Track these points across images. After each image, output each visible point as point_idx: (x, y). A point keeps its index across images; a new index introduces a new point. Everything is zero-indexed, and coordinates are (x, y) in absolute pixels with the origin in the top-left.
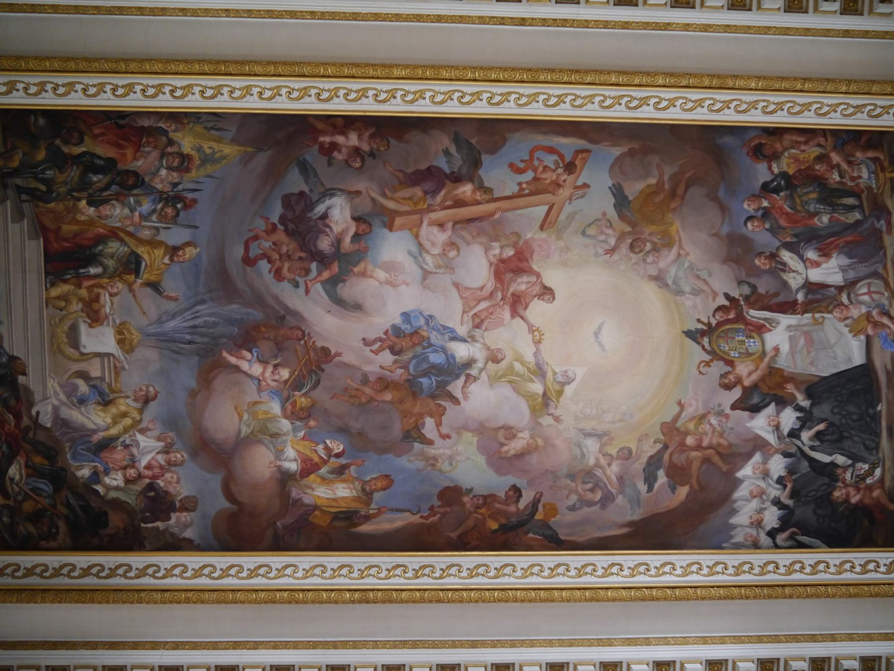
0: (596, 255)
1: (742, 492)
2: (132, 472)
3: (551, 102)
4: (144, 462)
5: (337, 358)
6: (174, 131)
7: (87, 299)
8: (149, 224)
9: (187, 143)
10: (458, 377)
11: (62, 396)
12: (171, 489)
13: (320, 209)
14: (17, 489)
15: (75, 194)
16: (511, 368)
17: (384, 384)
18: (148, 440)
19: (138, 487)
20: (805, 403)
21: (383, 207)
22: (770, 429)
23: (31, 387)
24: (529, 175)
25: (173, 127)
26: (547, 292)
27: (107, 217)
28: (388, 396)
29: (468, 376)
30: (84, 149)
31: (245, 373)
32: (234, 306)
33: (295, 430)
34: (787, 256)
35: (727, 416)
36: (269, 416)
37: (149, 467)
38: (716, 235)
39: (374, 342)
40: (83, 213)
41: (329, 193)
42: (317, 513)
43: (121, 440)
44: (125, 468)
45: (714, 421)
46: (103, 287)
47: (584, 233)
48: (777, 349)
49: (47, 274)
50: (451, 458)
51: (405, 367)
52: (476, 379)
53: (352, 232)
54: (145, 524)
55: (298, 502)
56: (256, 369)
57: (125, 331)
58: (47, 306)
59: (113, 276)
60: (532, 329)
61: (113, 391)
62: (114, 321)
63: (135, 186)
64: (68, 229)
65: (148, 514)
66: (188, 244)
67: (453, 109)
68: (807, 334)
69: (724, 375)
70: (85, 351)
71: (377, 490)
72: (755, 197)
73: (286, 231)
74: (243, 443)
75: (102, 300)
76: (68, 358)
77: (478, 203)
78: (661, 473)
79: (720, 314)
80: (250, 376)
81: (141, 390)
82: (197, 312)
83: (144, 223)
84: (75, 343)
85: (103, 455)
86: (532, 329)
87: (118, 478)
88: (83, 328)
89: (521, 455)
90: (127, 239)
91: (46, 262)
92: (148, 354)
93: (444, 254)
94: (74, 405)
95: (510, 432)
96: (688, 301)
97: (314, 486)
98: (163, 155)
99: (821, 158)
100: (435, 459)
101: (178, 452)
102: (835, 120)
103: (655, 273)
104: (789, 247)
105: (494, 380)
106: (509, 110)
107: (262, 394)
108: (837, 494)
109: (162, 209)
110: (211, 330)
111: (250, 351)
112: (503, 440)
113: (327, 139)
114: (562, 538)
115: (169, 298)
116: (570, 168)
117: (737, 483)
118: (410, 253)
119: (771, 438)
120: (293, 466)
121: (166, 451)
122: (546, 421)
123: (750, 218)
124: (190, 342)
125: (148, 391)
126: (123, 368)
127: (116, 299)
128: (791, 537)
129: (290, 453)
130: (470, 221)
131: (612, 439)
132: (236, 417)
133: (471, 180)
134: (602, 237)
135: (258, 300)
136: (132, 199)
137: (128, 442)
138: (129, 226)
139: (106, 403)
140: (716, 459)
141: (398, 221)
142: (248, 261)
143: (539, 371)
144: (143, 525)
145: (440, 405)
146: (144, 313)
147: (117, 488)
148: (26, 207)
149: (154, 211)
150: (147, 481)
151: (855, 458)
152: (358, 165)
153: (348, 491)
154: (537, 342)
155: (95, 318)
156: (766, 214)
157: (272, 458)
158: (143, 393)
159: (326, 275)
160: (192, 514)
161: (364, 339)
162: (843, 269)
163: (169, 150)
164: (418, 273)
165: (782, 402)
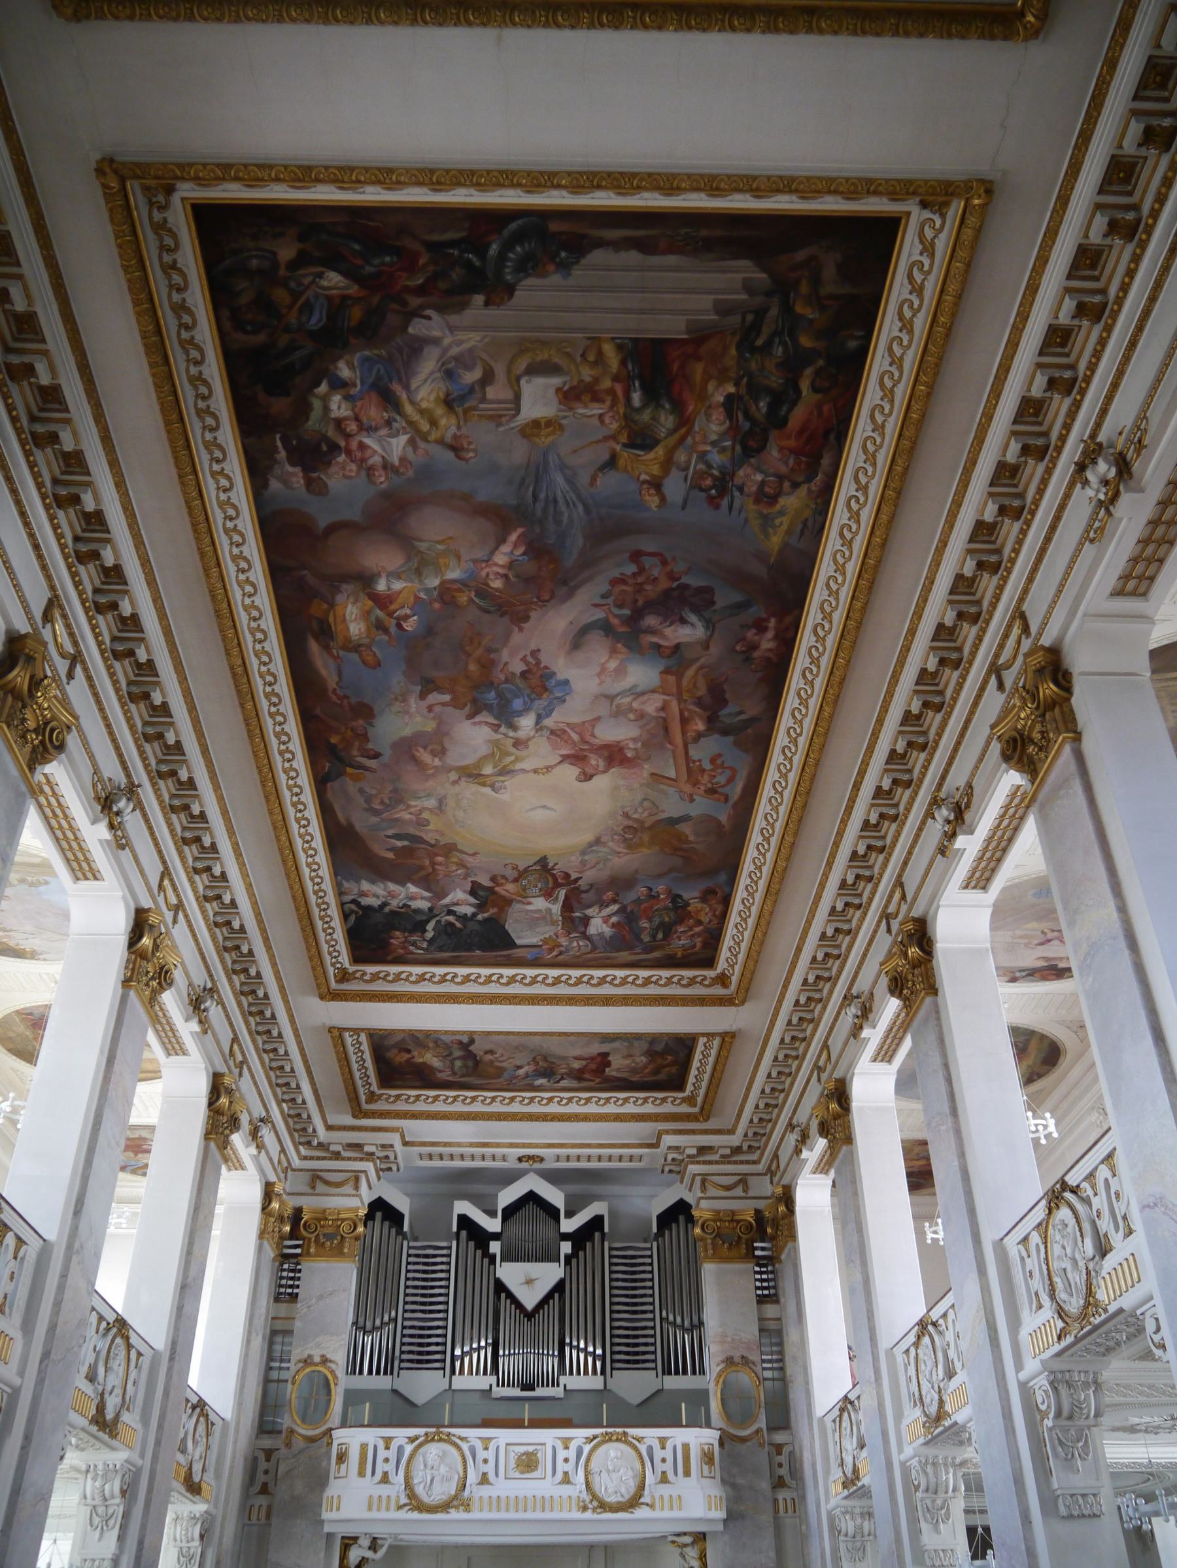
0: (623, 807)
1: (392, 886)
2: (352, 427)
3: (895, 347)
4: (368, 441)
5: (516, 629)
6: (809, 490)
7: (597, 388)
8: (694, 461)
9: (793, 502)
10: (496, 718)
11: (455, 351)
12: (333, 469)
13: (693, 618)
14: (306, 281)
15: (745, 380)
16: (509, 754)
17: (487, 665)
18: (400, 448)
19: (331, 433)
20: (480, 917)
21: (688, 667)
22: (455, 900)
23: (467, 311)
24: (707, 766)
25: (814, 488)
26: (587, 777)
27: (708, 416)
28: (472, 667)
29: (499, 726)
30: (805, 392)
31: (497, 548)
32: (580, 542)
33: (427, 591)
34: (615, 907)
35: (465, 878)
36: (443, 569)
37: (362, 446)
38: (636, 871)
39: (536, 658)
40: (717, 388)
41: (709, 624)
42: (325, 606)
43: (398, 418)
44: (357, 419)
45: (459, 872)
46: (612, 407)
47: (645, 799)
48: (529, 903)
49: (635, 341)
50: (407, 712)
51: (507, 681)
52: (496, 731)
53: (662, 642)
54: (281, 439)
55: (338, 590)
56: (501, 558)
57: (551, 429)
58: (589, 338)
59: (628, 420)
60: (548, 769)
61: (466, 412)
62: (565, 417)
63: (745, 448)
64: (698, 369)
65: (294, 442)
66: (663, 499)
67: (785, 721)
68: (544, 918)
69: (504, 877)
70: (523, 382)
71: (361, 656)
72: (669, 892)
73: (671, 589)
74: (407, 543)
75: (596, 405)
76: (512, 361)
77: (684, 733)
78: (406, 843)
79: (562, 875)
80: (492, 553)
81: (470, 443)
82: (574, 505)
83: (695, 456)
84: (534, 370)
85: (374, 395)
86: (548, 769)
87: (342, 411)
88: (556, 381)
89: (415, 760)
90: (676, 436)
91: (652, 340)
92: (519, 453)
93: (631, 710)
94: (443, 365)
95: (441, 752)
96: (575, 860)
97: (359, 604)
98: (781, 478)
99: (700, 923)
100: (404, 701)
101: (387, 478)
102: (730, 931)
103: (603, 840)
104: (622, 910)
105: (496, 744)
106: (776, 757)
107: (471, 564)
108: (397, 933)
109: (712, 475)
110: (551, 518)
111: (524, 554)
112: (430, 748)
113: (772, 623)
114: (329, 785)
115: (593, 479)
116: (712, 791)
117: (402, 883)
118: (635, 686)
119: (447, 901)
120: (381, 586)
121: (386, 466)
122: (453, 776)
123: (650, 889)
124: (535, 497)
125: (468, 451)
126: (499, 425)
127: (595, 422)
128: (352, 911)
129: (397, 585)
130: (666, 729)
131: (437, 815)
132: (440, 538)
133: (707, 730)
134: (640, 810)
135: (588, 563)
136: (728, 443)
137: (395, 425)
138: (694, 438)
139: (449, 403)
140: (422, 873)
141: (671, 679)
142: (636, 556)
143: (505, 772)
144: (278, 436)
145: (465, 705)
146: (575, 451)
147: (326, 409)
148: (735, 320)
149: (710, 466)
150: (343, 444)
151: (431, 942)
152: (738, 648)
153: (357, 632)
154: (535, 771)
155: (569, 396)
156: (652, 896)
157: (391, 568)
158: (465, 446)
159: (615, 621)
160: (303, 489)
161: (539, 650)
162: (601, 935)
163: (787, 484)
164: (614, 692)
165: (481, 907)
